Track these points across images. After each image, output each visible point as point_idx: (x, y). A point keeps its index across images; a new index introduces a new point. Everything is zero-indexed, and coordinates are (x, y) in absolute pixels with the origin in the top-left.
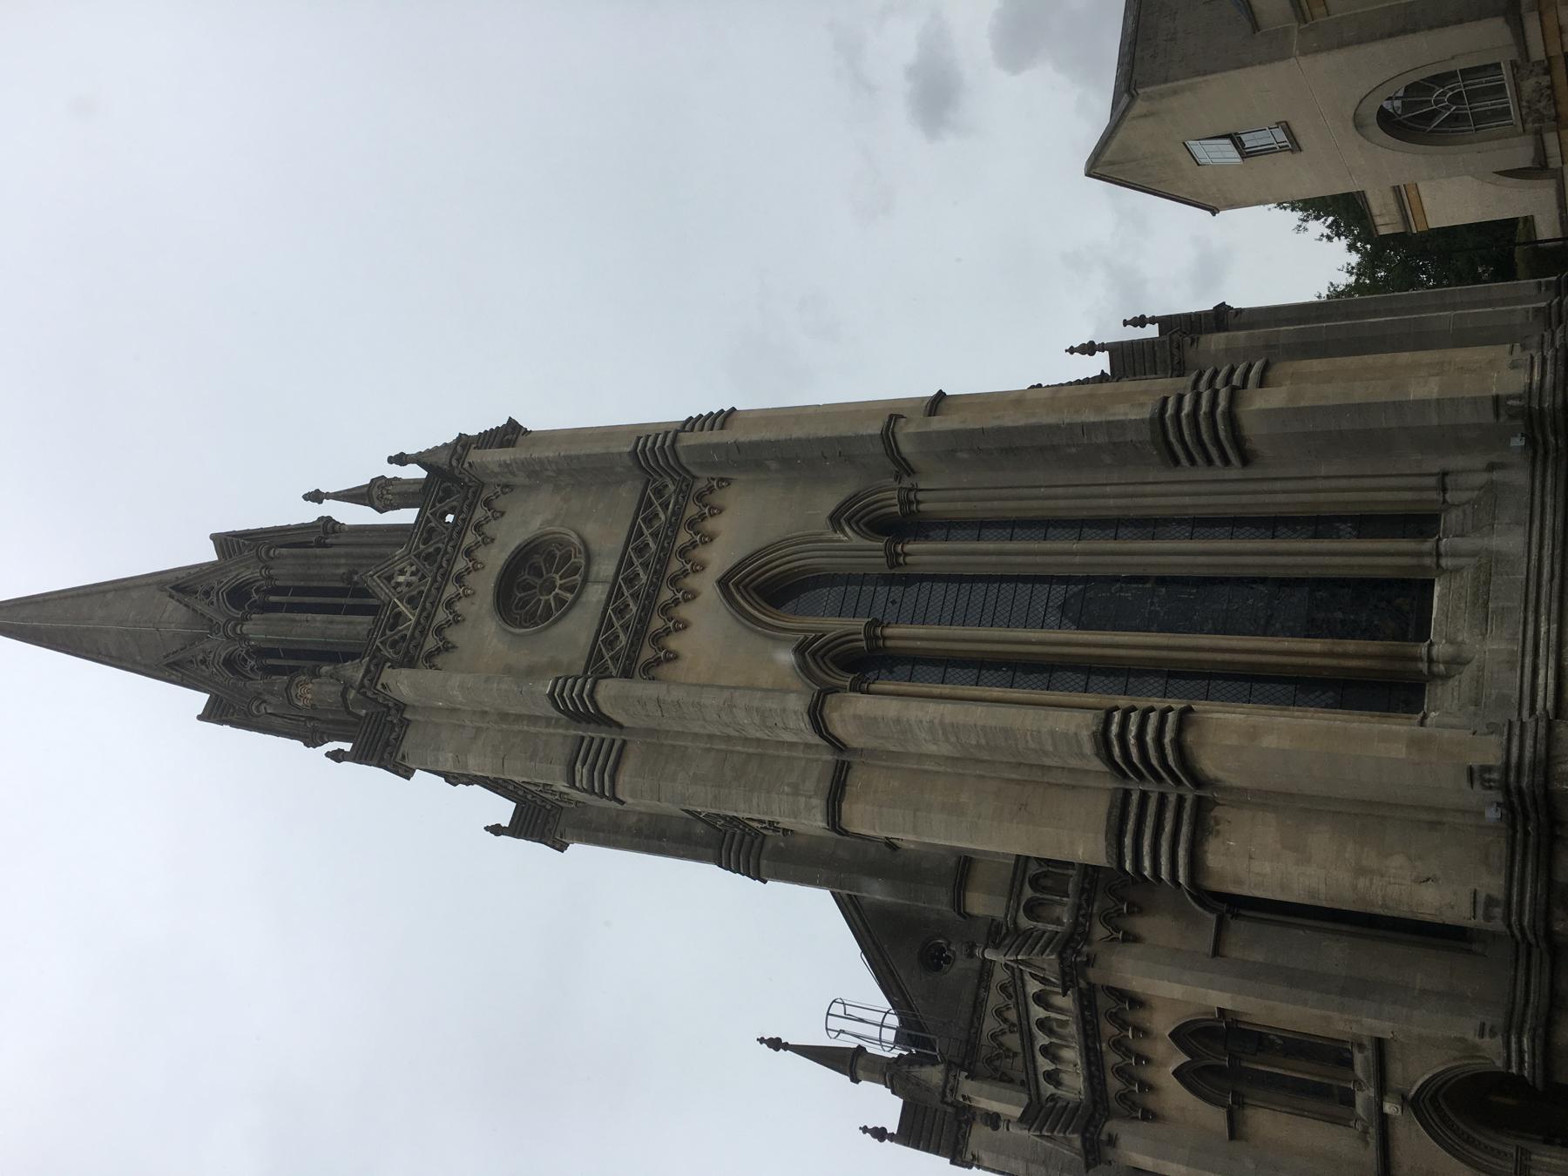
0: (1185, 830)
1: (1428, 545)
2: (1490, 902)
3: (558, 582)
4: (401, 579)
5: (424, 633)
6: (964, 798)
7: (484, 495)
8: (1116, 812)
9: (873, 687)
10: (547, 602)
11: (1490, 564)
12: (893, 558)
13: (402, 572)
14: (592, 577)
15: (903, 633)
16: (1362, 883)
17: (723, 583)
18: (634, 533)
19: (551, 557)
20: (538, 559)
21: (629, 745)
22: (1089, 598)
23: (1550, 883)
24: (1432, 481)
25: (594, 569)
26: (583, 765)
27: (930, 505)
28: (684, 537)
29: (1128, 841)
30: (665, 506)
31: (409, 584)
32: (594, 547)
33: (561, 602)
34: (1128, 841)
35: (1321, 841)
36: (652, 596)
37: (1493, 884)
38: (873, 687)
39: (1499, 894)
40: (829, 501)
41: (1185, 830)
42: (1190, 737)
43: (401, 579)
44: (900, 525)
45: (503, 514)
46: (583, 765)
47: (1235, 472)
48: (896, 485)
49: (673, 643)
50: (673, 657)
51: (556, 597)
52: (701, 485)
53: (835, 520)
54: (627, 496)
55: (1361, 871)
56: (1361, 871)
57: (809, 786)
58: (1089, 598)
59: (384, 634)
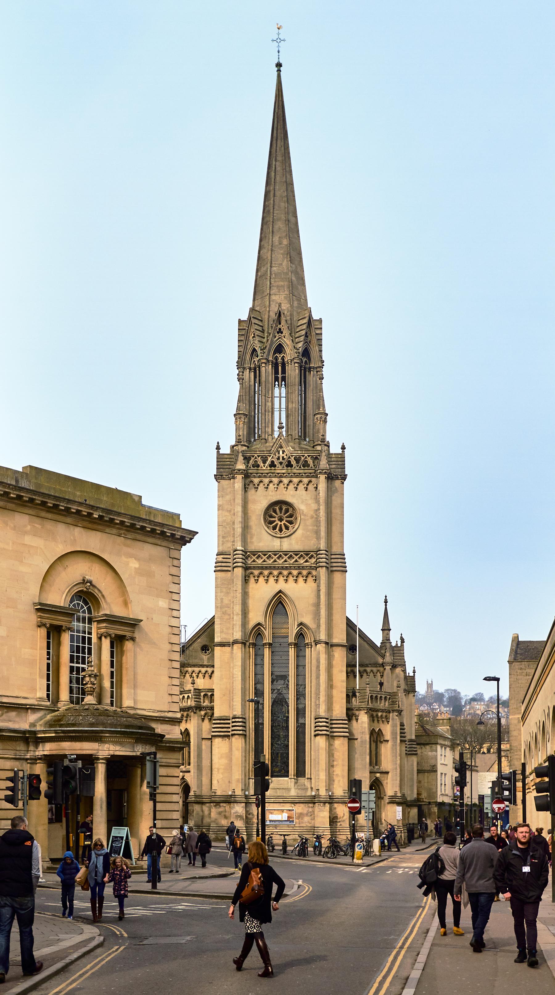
0: (222, 734)
1: (293, 777)
2: (215, 793)
3: (282, 523)
4: (281, 452)
5: (259, 477)
6: (225, 680)
7: (313, 480)
8: (225, 718)
9: (251, 649)
10: (275, 521)
11: (288, 790)
12: (290, 644)
13: (283, 452)
14: (282, 540)
15: (267, 652)
16: (216, 770)
17: (280, 591)
18: (296, 553)
19: (291, 516)
20: (291, 510)
21: (229, 573)
22: (279, 703)
23: (220, 803)
24: (309, 777)
25: (285, 539)
26: (223, 558)
27: (308, 651)
28: (295, 572)
29: (218, 721)
30: (307, 561)
31: (278, 459)
32: (293, 536)
33: (274, 528)
34: (218, 721)
35: (224, 761)
37: (219, 793)
38: (251, 649)
39: (217, 794)
40: (308, 620)
41: (222, 734)
42: (236, 736)
43: (281, 452)
44: (301, 642)
45: (306, 490)
46: (223, 558)
47: (313, 733)
48: (312, 641)
49: (261, 579)
50: (257, 581)
51: (277, 524)
52: (314, 573)
53: (301, 624)
54: (310, 545)
55: (218, 769)
56: (218, 769)
57: (224, 636)
58: (279, 703)
59: (259, 456)
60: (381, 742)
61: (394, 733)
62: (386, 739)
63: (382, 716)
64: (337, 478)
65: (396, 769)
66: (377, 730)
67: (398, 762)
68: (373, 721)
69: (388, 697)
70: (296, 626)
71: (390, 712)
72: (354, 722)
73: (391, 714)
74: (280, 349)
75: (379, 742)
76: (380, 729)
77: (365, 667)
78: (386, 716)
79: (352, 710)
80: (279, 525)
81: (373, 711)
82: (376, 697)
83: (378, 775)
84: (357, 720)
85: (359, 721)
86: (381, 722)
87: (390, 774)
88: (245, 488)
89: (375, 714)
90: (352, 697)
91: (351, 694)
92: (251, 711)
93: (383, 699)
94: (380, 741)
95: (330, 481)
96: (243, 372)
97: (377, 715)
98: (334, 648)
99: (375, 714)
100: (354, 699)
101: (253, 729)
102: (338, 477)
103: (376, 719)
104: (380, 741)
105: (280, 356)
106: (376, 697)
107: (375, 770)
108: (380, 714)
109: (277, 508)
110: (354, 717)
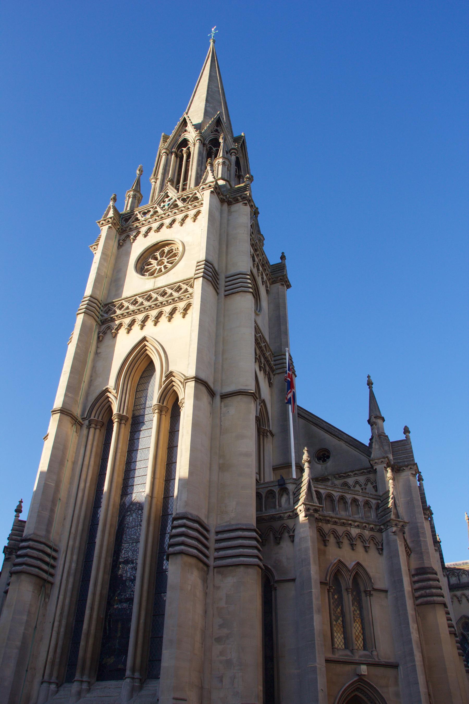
14: (157, 279)
17: (144, 339)
36: (140, 311)
38: (92, 430)
60: (368, 593)
61: (395, 572)
62: (379, 585)
63: (360, 536)
64: (237, 201)
65: (412, 654)
66: (351, 565)
67: (415, 636)
68: (339, 544)
69: (374, 501)
70: (164, 379)
71: (380, 531)
72: (286, 545)
73: (384, 534)
74: (185, 143)
75: (363, 595)
76: (358, 564)
77: (344, 477)
78: (373, 538)
79: (281, 518)
80: (154, 268)
81: (335, 523)
82: (342, 498)
83: (364, 669)
84: (292, 538)
85: (296, 540)
86: (360, 548)
87: (401, 668)
88: (119, 244)
89: (340, 530)
90: (281, 495)
91: (276, 489)
92: (72, 536)
93: (361, 504)
94: (365, 591)
95: (225, 206)
96: (156, 183)
97: (348, 534)
98: (228, 401)
99: (340, 530)
100: (284, 499)
101: (72, 571)
102: (237, 200)
103: (346, 542)
104: (365, 591)
105: (185, 149)
106: (342, 498)
107: (357, 658)
108: (354, 532)
109: (158, 254)
110: (286, 535)
